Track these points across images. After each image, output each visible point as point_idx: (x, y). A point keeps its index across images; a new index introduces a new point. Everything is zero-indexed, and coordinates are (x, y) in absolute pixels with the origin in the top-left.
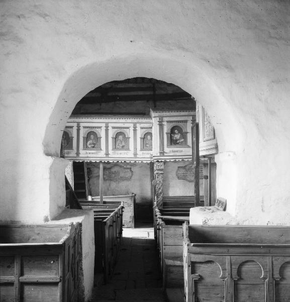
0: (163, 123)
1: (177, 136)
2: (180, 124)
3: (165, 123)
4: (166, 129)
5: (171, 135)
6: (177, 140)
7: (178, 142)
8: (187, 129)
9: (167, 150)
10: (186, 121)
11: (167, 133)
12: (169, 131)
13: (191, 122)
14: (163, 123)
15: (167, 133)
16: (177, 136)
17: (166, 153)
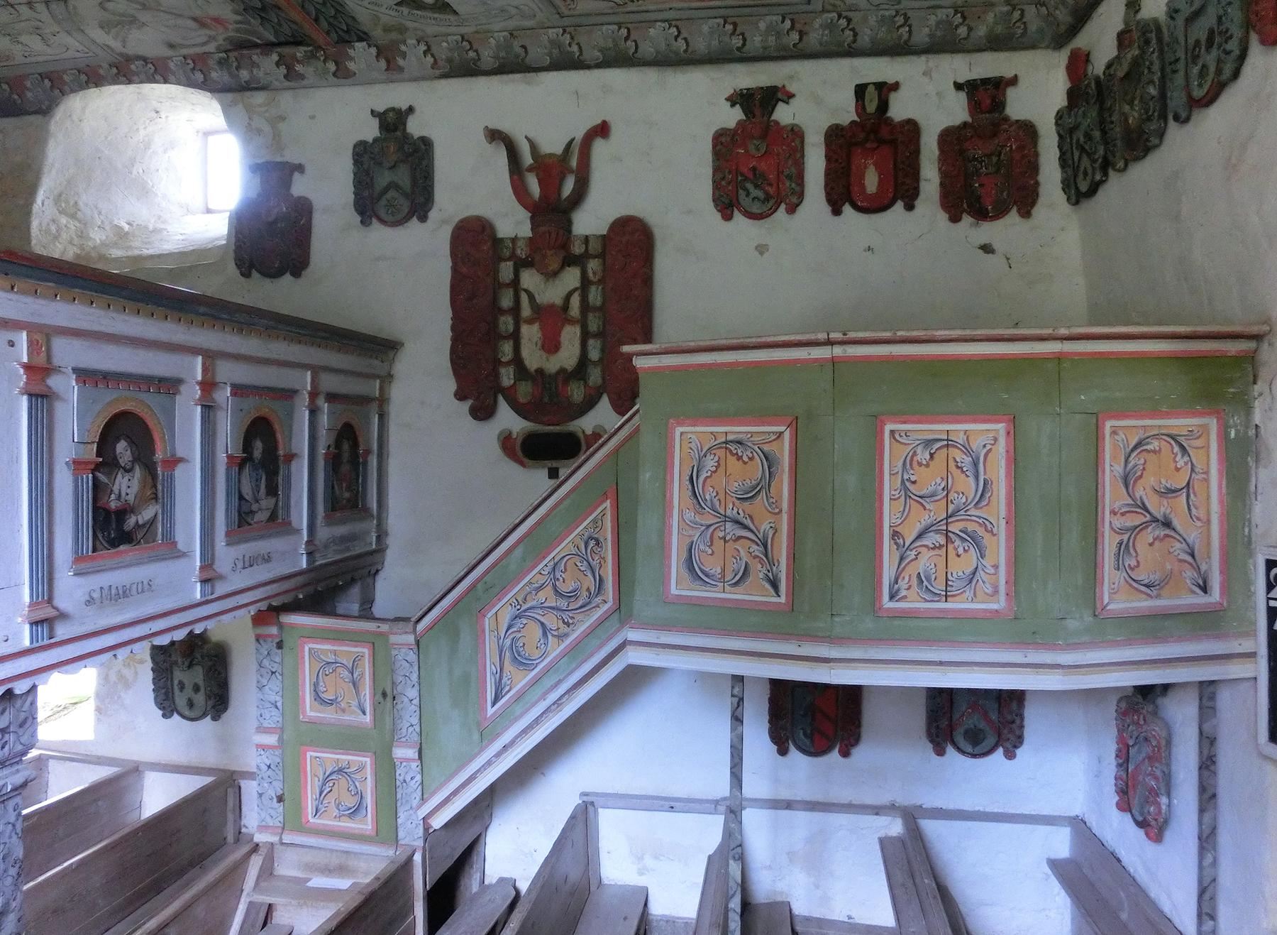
0: (54, 382)
1: (126, 486)
2: (146, 405)
3: (67, 388)
4: (73, 429)
5: (97, 485)
6: (123, 513)
7: (131, 521)
8: (173, 448)
9: (71, 589)
10: (169, 386)
11: (77, 465)
12: (91, 453)
13: (198, 393)
14: (54, 382)
15: (77, 465)
16: (126, 486)
17: (63, 616)
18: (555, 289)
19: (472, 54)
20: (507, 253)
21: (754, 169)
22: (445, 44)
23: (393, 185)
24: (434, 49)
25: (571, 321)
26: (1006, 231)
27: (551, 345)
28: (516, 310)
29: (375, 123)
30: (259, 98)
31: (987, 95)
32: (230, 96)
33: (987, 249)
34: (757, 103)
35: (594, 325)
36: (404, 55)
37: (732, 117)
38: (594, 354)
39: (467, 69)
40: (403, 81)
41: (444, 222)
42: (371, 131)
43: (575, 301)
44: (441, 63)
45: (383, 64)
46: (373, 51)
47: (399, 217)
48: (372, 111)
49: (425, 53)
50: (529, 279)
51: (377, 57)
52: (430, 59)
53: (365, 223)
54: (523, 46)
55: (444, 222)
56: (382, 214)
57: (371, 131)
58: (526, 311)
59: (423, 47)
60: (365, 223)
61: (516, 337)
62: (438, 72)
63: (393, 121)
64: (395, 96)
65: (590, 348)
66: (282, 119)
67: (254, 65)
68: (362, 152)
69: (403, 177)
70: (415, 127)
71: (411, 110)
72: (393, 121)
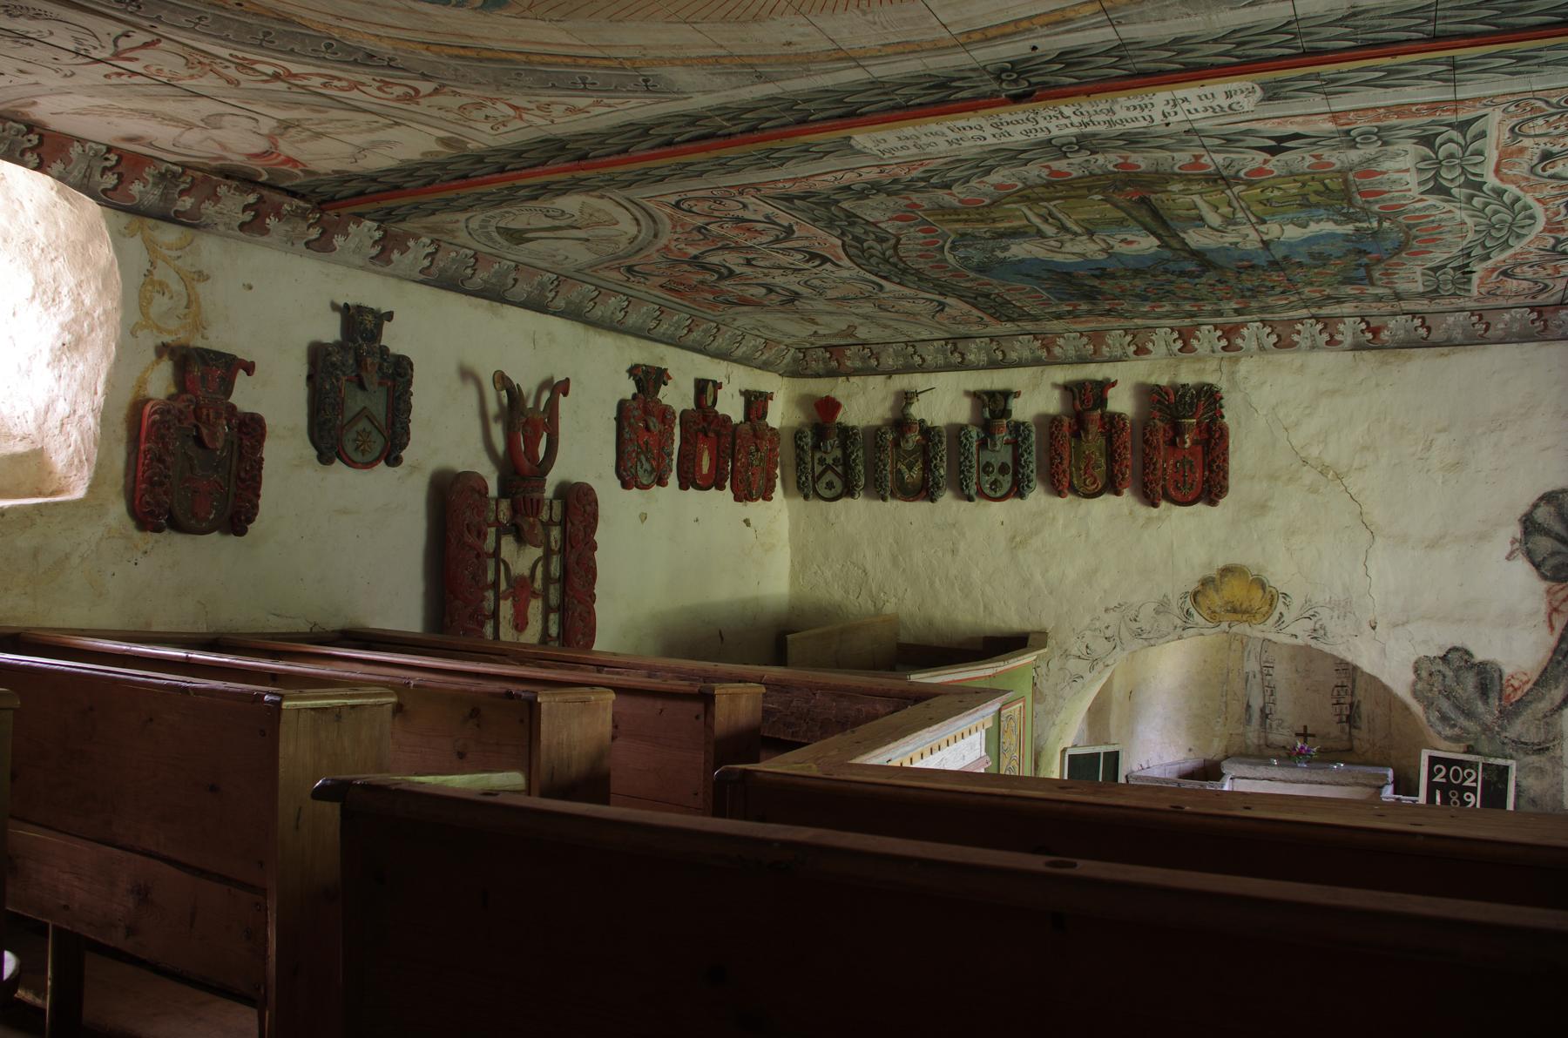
18: (522, 560)
19: (469, 271)
20: (492, 518)
21: (647, 443)
22: (453, 254)
23: (364, 413)
24: (439, 255)
25: (535, 595)
26: (756, 509)
27: (520, 624)
28: (496, 584)
29: (336, 318)
30: (170, 234)
31: (756, 402)
32: (124, 219)
33: (747, 522)
34: (649, 379)
35: (554, 598)
36: (404, 250)
37: (628, 388)
38: (554, 630)
39: (450, 283)
40: (386, 275)
41: (414, 468)
42: (330, 331)
43: (539, 570)
44: (433, 269)
45: (375, 251)
46: (378, 235)
47: (369, 458)
48: (563, 387)
49: (428, 255)
50: (508, 547)
51: (375, 243)
52: (427, 263)
53: (325, 458)
54: (516, 280)
55: (414, 468)
56: (349, 448)
57: (330, 331)
58: (503, 586)
59: (431, 249)
60: (325, 458)
61: (495, 615)
62: (422, 277)
63: (361, 324)
64: (369, 290)
65: (551, 623)
66: (202, 276)
67: (216, 198)
68: (318, 355)
69: (375, 401)
70: (395, 339)
71: (389, 316)
72: (361, 324)
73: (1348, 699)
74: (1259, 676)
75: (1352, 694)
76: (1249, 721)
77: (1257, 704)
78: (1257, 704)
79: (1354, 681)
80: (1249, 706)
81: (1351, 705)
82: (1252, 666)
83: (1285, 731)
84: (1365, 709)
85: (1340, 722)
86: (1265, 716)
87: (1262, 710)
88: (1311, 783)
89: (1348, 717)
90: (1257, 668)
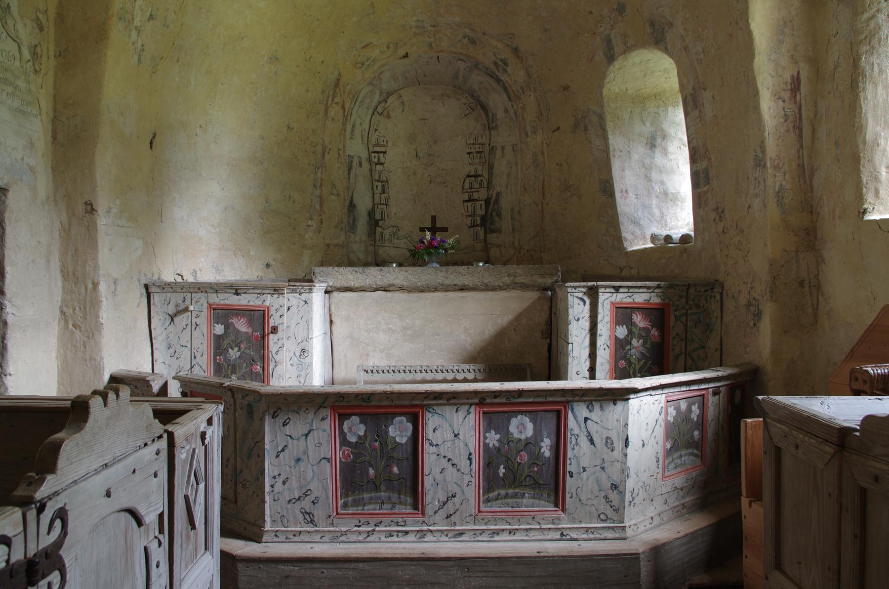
73: (483, 194)
74: (365, 164)
75: (489, 186)
76: (352, 227)
77: (364, 203)
78: (364, 203)
79: (491, 168)
80: (352, 206)
81: (487, 201)
82: (357, 148)
83: (402, 243)
84: (506, 203)
85: (473, 225)
86: (374, 222)
87: (371, 214)
88: (446, 288)
89: (483, 218)
90: (364, 155)
